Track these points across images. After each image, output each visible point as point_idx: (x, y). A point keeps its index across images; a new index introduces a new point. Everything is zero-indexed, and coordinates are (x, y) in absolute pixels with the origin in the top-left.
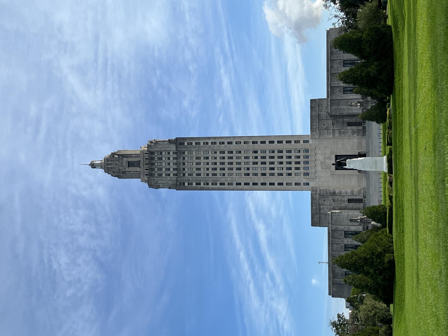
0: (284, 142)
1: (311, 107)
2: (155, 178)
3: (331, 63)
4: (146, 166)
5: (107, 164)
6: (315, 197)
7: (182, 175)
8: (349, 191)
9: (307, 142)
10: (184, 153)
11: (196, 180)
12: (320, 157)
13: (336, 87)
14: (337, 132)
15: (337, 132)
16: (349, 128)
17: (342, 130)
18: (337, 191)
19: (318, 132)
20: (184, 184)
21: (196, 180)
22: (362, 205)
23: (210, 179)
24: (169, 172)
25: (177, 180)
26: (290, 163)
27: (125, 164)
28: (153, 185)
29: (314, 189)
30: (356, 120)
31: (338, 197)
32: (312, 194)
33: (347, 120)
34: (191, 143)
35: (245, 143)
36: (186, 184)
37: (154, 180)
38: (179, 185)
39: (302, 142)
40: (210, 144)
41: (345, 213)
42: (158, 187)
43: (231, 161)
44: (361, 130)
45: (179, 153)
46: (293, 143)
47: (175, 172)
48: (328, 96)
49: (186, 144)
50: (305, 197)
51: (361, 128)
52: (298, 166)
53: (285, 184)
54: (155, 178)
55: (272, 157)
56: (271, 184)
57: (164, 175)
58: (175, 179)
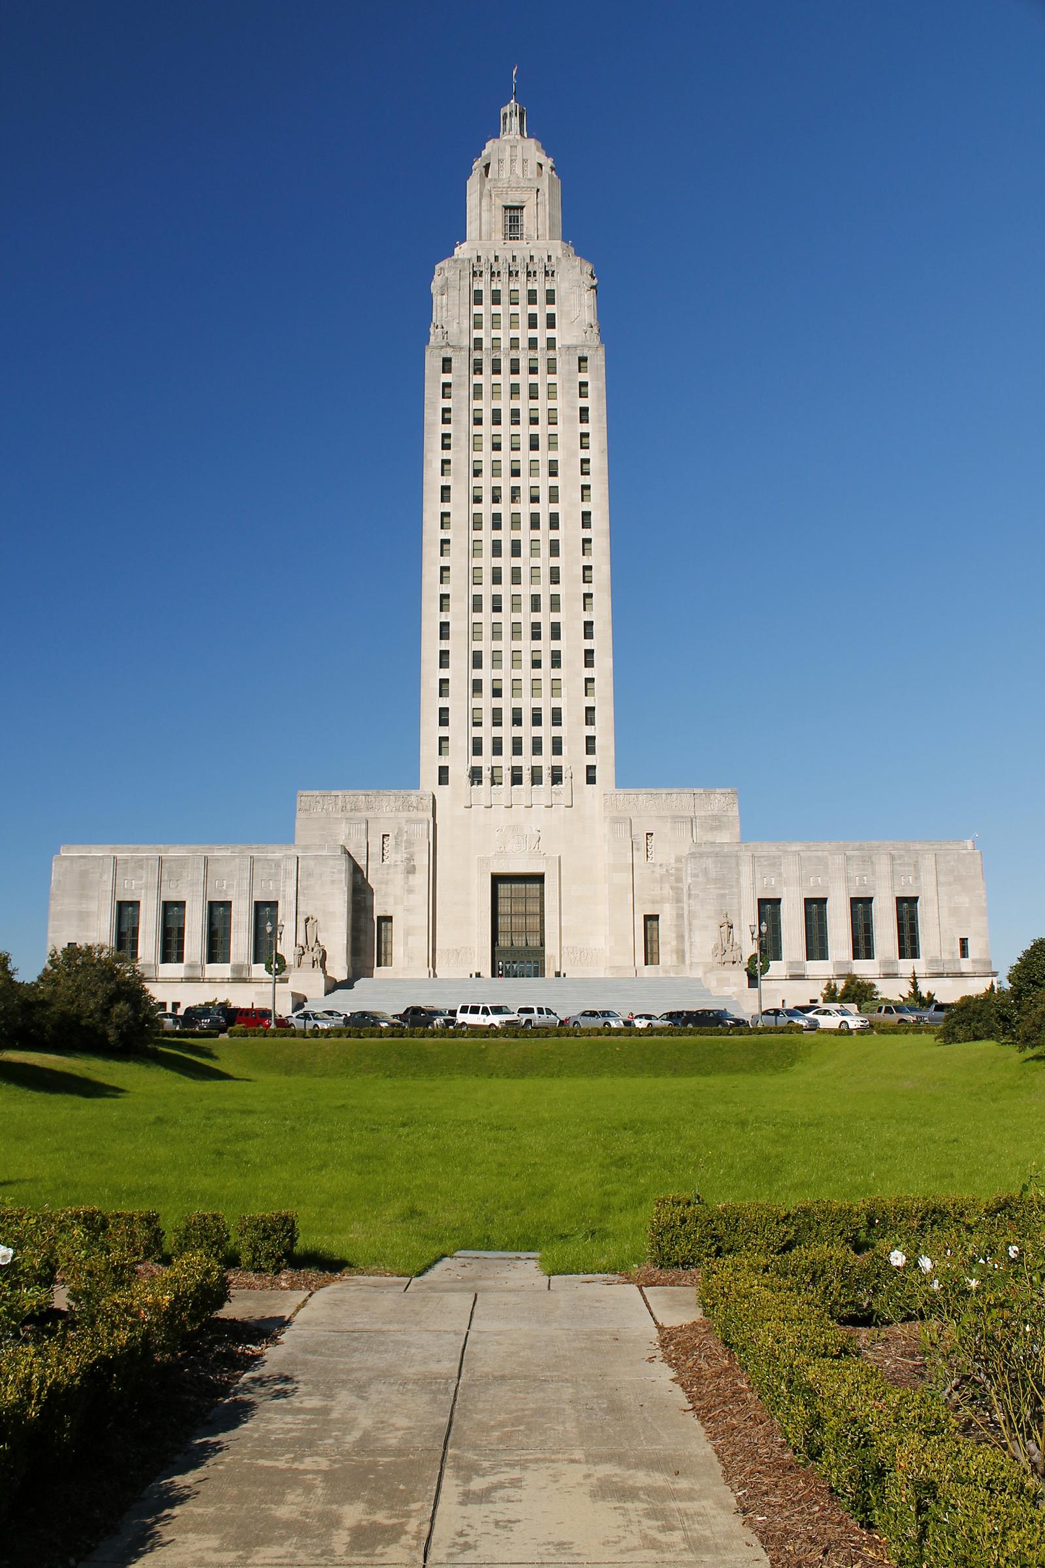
9: (591, 780)
13: (780, 875)
25: (461, 348)
26: (517, 721)
27: (512, 199)
43: (525, 522)
46: (589, 731)
52: (507, 747)
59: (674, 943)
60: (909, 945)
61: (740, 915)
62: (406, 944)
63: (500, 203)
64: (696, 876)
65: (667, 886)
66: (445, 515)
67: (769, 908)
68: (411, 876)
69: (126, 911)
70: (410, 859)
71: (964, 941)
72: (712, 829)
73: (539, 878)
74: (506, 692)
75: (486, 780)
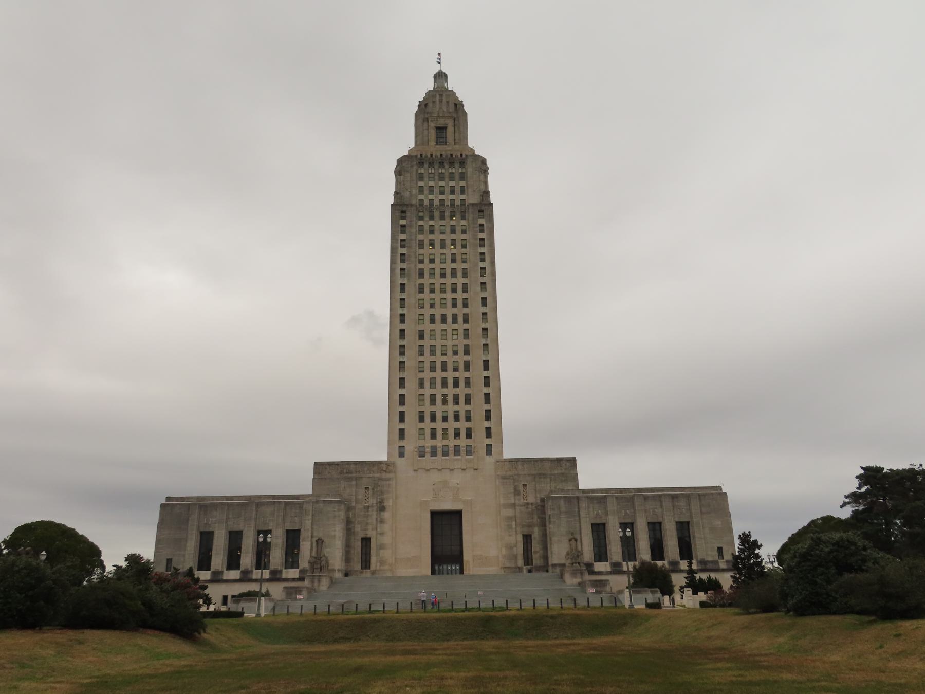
0: (487, 407)
1: (559, 460)
2: (415, 168)
3: (654, 496)
4: (439, 155)
5: (441, 95)
6: (375, 468)
7: (421, 214)
8: (386, 540)
10: (463, 218)
11: (411, 240)
12: (456, 479)
13: (605, 508)
14: (509, 512)
15: (509, 512)
16: (520, 538)
17: (514, 523)
18: (386, 515)
19: (509, 473)
20: (403, 218)
21: (411, 240)
22: (358, 567)
23: (412, 266)
24: (426, 192)
25: (411, 205)
27: (441, 123)
28: (403, 166)
29: (391, 468)
30: (536, 552)
31: (374, 517)
32: (380, 462)
33: (536, 533)
34: (482, 231)
35: (485, 330)
36: (403, 222)
37: (412, 166)
38: (400, 208)
39: (488, 441)
40: (481, 265)
41: (337, 531)
42: (399, 172)
44: (516, 563)
45: (462, 210)
46: (487, 424)
47: (426, 203)
48: (584, 491)
49: (481, 221)
50: (373, 447)
51: (520, 562)
53: (402, 408)
54: (415, 168)
55: (456, 384)
56: (402, 380)
57: (421, 184)
58: (414, 202)
59: (541, 552)
60: (686, 550)
61: (581, 534)
62: (377, 554)
63: (432, 125)
64: (553, 509)
65: (536, 517)
66: (403, 300)
67: (599, 530)
68: (382, 513)
69: (206, 539)
70: (382, 502)
71: (720, 550)
72: (562, 481)
73: (459, 513)
74: (437, 260)
75: (428, 456)
